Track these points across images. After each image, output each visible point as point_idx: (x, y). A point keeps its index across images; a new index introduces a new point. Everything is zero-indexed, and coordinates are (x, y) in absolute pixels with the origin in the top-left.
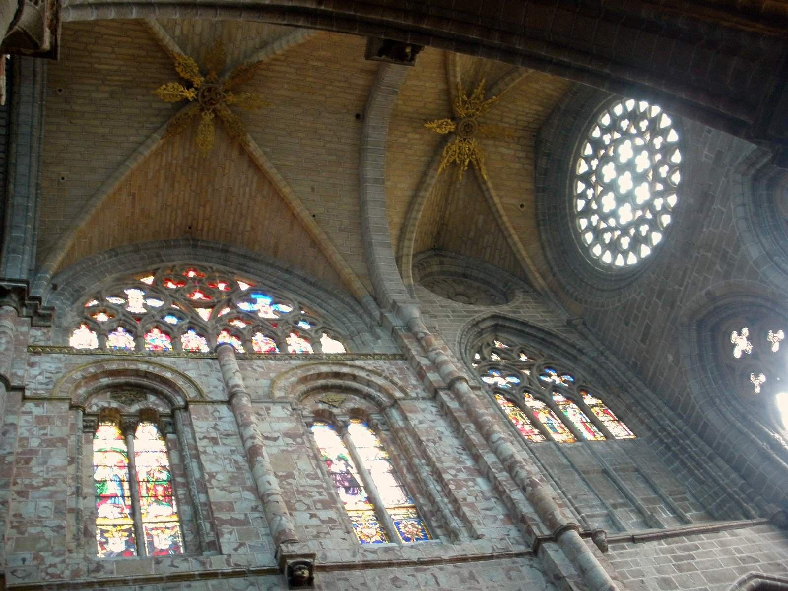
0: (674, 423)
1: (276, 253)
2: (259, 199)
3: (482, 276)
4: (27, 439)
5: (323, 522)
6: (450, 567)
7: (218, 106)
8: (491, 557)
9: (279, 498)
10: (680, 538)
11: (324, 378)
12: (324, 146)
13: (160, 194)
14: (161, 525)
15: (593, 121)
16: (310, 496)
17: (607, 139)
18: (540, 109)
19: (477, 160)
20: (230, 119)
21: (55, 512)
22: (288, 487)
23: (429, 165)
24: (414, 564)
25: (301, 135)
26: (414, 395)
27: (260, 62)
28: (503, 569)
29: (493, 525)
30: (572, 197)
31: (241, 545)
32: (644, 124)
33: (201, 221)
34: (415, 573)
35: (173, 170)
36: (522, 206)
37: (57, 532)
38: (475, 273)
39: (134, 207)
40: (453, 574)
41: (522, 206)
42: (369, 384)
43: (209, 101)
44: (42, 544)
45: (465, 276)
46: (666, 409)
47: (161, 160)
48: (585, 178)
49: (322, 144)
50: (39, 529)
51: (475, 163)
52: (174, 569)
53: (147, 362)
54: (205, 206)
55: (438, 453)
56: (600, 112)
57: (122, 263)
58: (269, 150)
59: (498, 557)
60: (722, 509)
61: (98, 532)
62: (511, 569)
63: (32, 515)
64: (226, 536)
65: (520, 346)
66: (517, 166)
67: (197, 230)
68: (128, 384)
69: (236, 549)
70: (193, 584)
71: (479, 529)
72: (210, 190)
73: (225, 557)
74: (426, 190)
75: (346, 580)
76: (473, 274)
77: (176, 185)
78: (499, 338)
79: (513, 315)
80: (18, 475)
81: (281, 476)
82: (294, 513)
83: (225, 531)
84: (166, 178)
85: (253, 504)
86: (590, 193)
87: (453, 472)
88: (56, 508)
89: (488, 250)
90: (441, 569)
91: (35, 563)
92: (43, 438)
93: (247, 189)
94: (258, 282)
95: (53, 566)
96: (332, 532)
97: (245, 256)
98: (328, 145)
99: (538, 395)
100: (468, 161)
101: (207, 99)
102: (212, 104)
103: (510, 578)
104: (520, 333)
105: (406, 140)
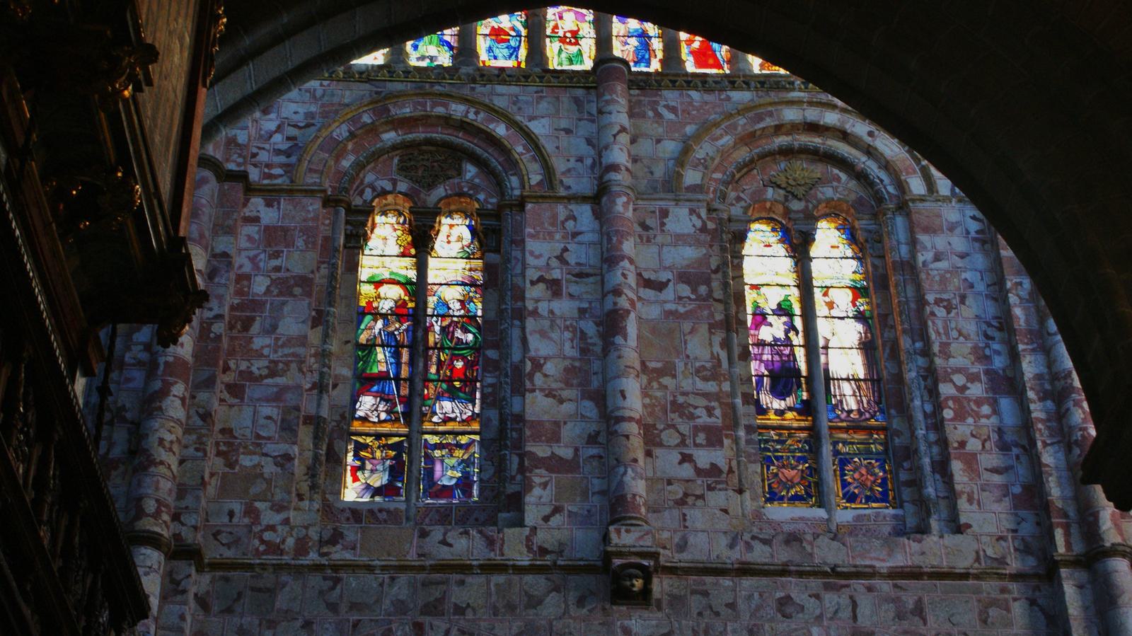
4: (248, 277)
5: (699, 472)
6: (885, 586)
8: (964, 576)
9: (633, 428)
11: (787, 134)
14: (450, 439)
16: (692, 417)
21: (283, 429)
22: (659, 394)
24: (825, 574)
28: (979, 601)
29: (997, 507)
31: (557, 510)
34: (822, 593)
37: (282, 466)
40: (888, 600)
44: (256, 489)
50: (256, 459)
52: (446, 548)
55: (947, 334)
61: (351, 447)
62: (993, 603)
63: (248, 433)
64: (537, 491)
69: (546, 519)
70: (469, 579)
71: (966, 512)
73: (527, 531)
75: (705, 594)
80: (231, 353)
81: (654, 370)
82: (657, 451)
83: (537, 480)
85: (593, 427)
87: (959, 379)
88: (283, 420)
90: (870, 589)
91: (246, 521)
92: (274, 275)
95: (272, 528)
96: (709, 495)
103: (985, 622)
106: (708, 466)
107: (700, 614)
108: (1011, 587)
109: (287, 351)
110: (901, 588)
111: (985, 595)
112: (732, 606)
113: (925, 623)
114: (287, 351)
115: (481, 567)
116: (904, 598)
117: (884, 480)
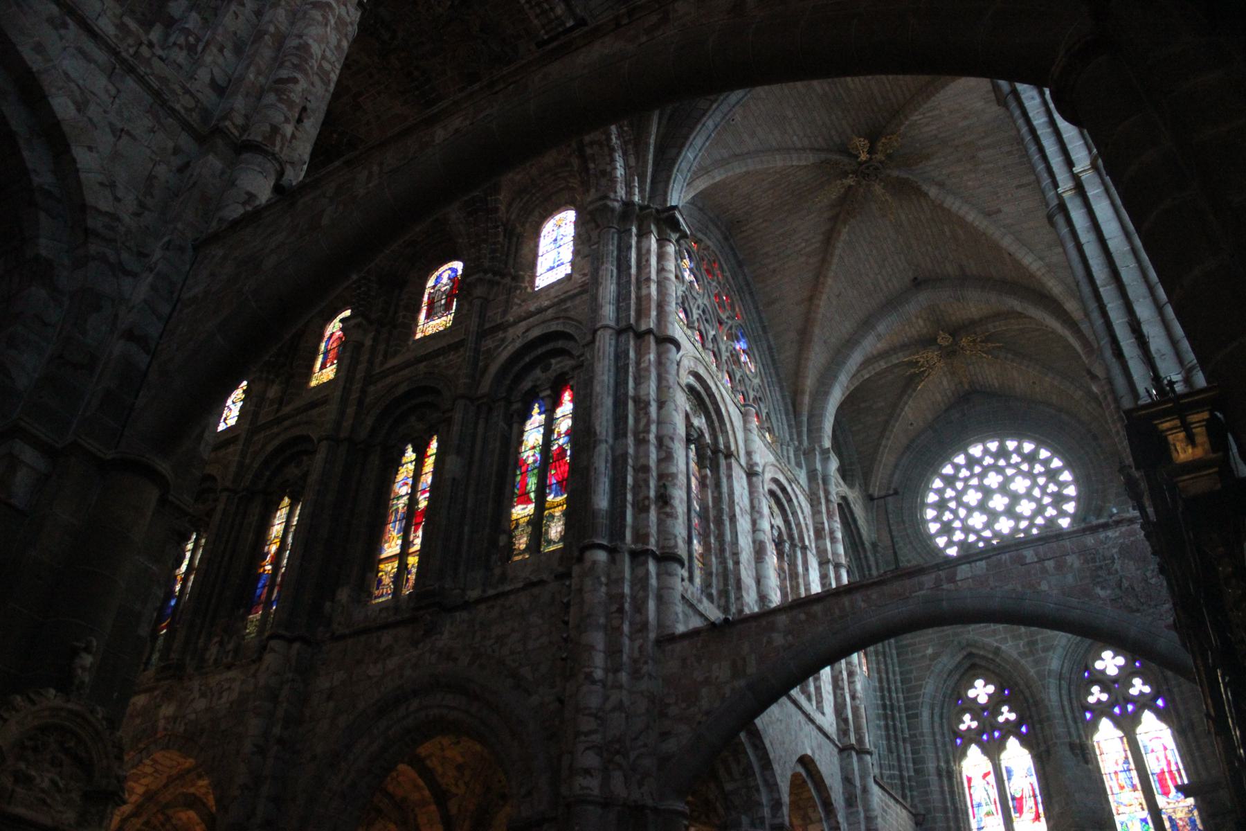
0: (897, 693)
15: (1020, 436)
17: (1015, 459)
18: (997, 385)
19: (929, 374)
25: (874, 251)
27: (926, 195)
30: (946, 458)
32: (1052, 488)
41: (912, 424)
42: (794, 513)
46: (898, 678)
48: (971, 462)
56: (1031, 439)
66: (939, 397)
86: (964, 473)
93: (803, 245)
97: (748, 284)
98: (879, 277)
101: (867, 171)
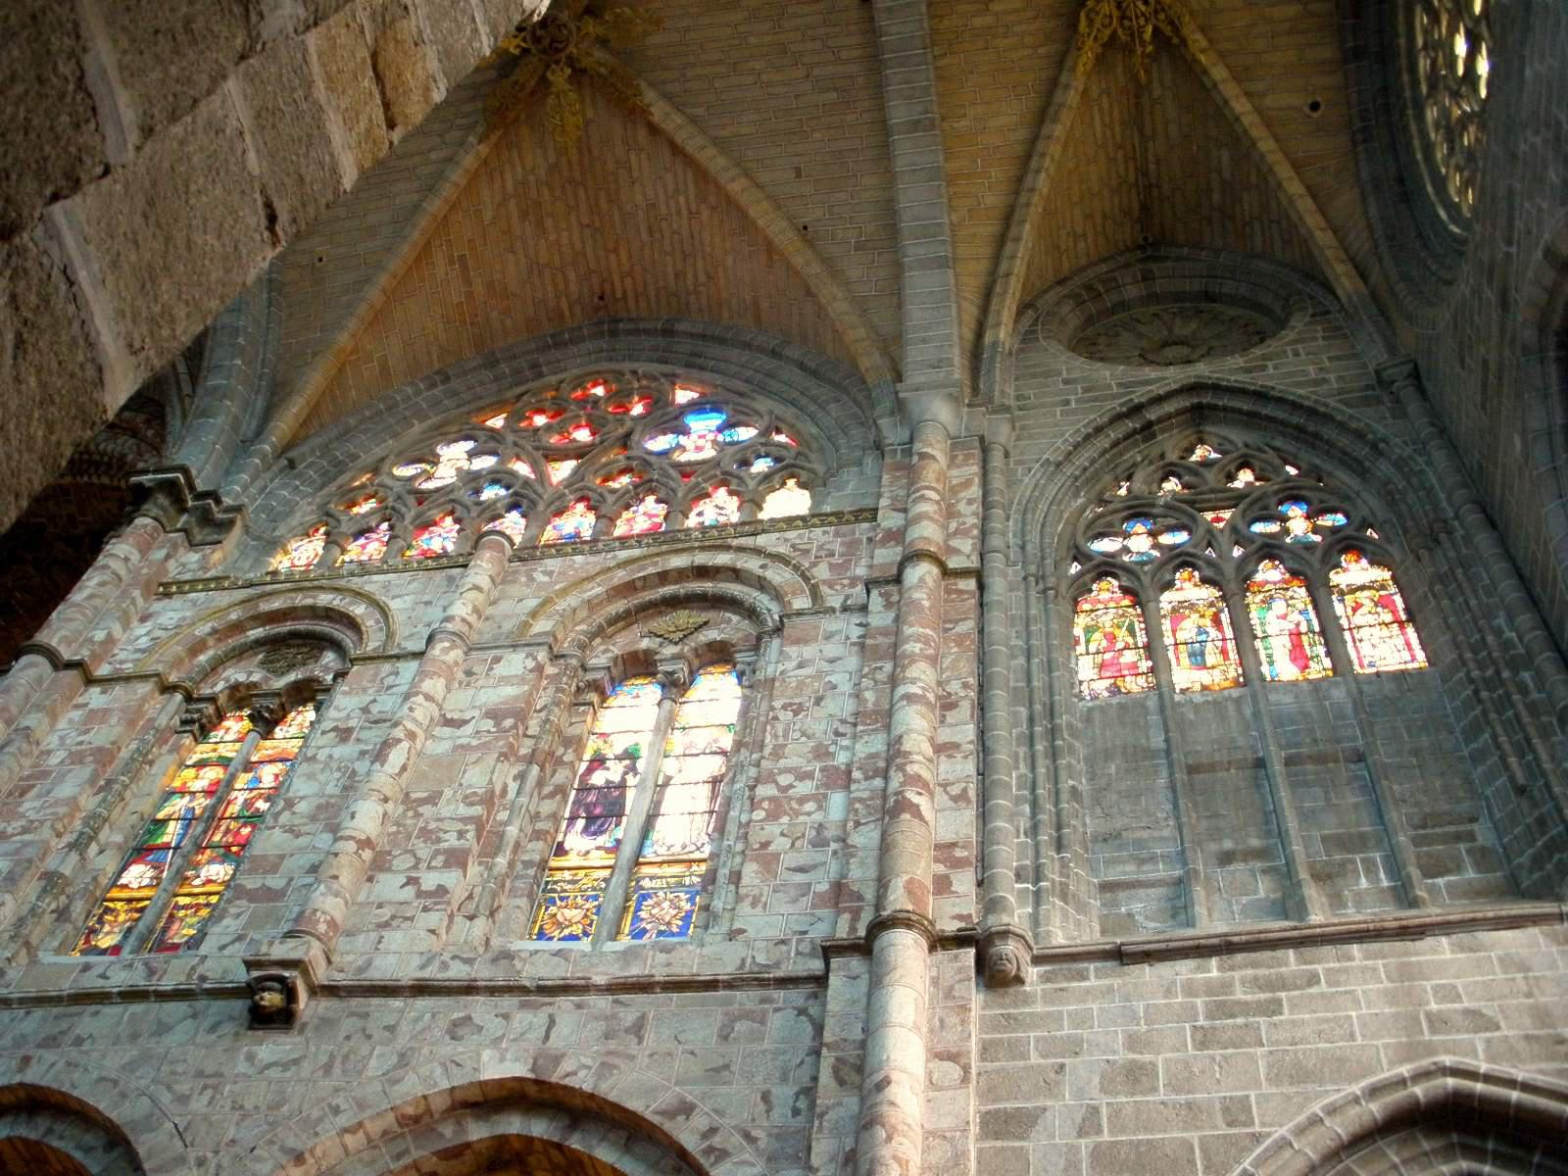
1: (758, 318)
2: (705, 215)
3: (1244, 290)
6: (602, 1003)
7: (572, 49)
10: (1279, 953)
11: (676, 582)
12: (808, 76)
13: (519, 244)
19: (1171, 23)
20: (603, 70)
23: (1060, 62)
25: (757, 65)
26: (835, 602)
33: (616, 278)
35: (534, 194)
36: (1315, 106)
38: (1228, 287)
39: (468, 282)
43: (551, 44)
45: (1209, 297)
47: (503, 181)
49: (802, 72)
51: (1168, 30)
53: (337, 590)
54: (616, 250)
55: (786, 736)
57: (455, 394)
58: (700, 111)
59: (730, 985)
60: (1541, 869)
65: (1244, 450)
67: (616, 300)
68: (294, 634)
72: (616, 217)
74: (1055, 120)
76: (1225, 290)
77: (549, 222)
78: (1206, 437)
79: (1241, 377)
84: (524, 215)
89: (1257, 226)
90: (579, 1006)
93: (682, 199)
94: (716, 386)
97: (703, 337)
98: (816, 72)
99: (1209, 573)
100: (1149, 29)
101: (546, 42)
102: (558, 51)
104: (1251, 420)
105: (988, 20)
106: (433, 888)
107: (348, 1038)
108: (776, 996)
109: (48, 811)
110: (622, 1003)
111: (736, 1006)
112: (391, 1029)
113: (640, 1040)
114: (48, 811)
115: (122, 995)
116: (621, 1015)
117: (689, 914)
